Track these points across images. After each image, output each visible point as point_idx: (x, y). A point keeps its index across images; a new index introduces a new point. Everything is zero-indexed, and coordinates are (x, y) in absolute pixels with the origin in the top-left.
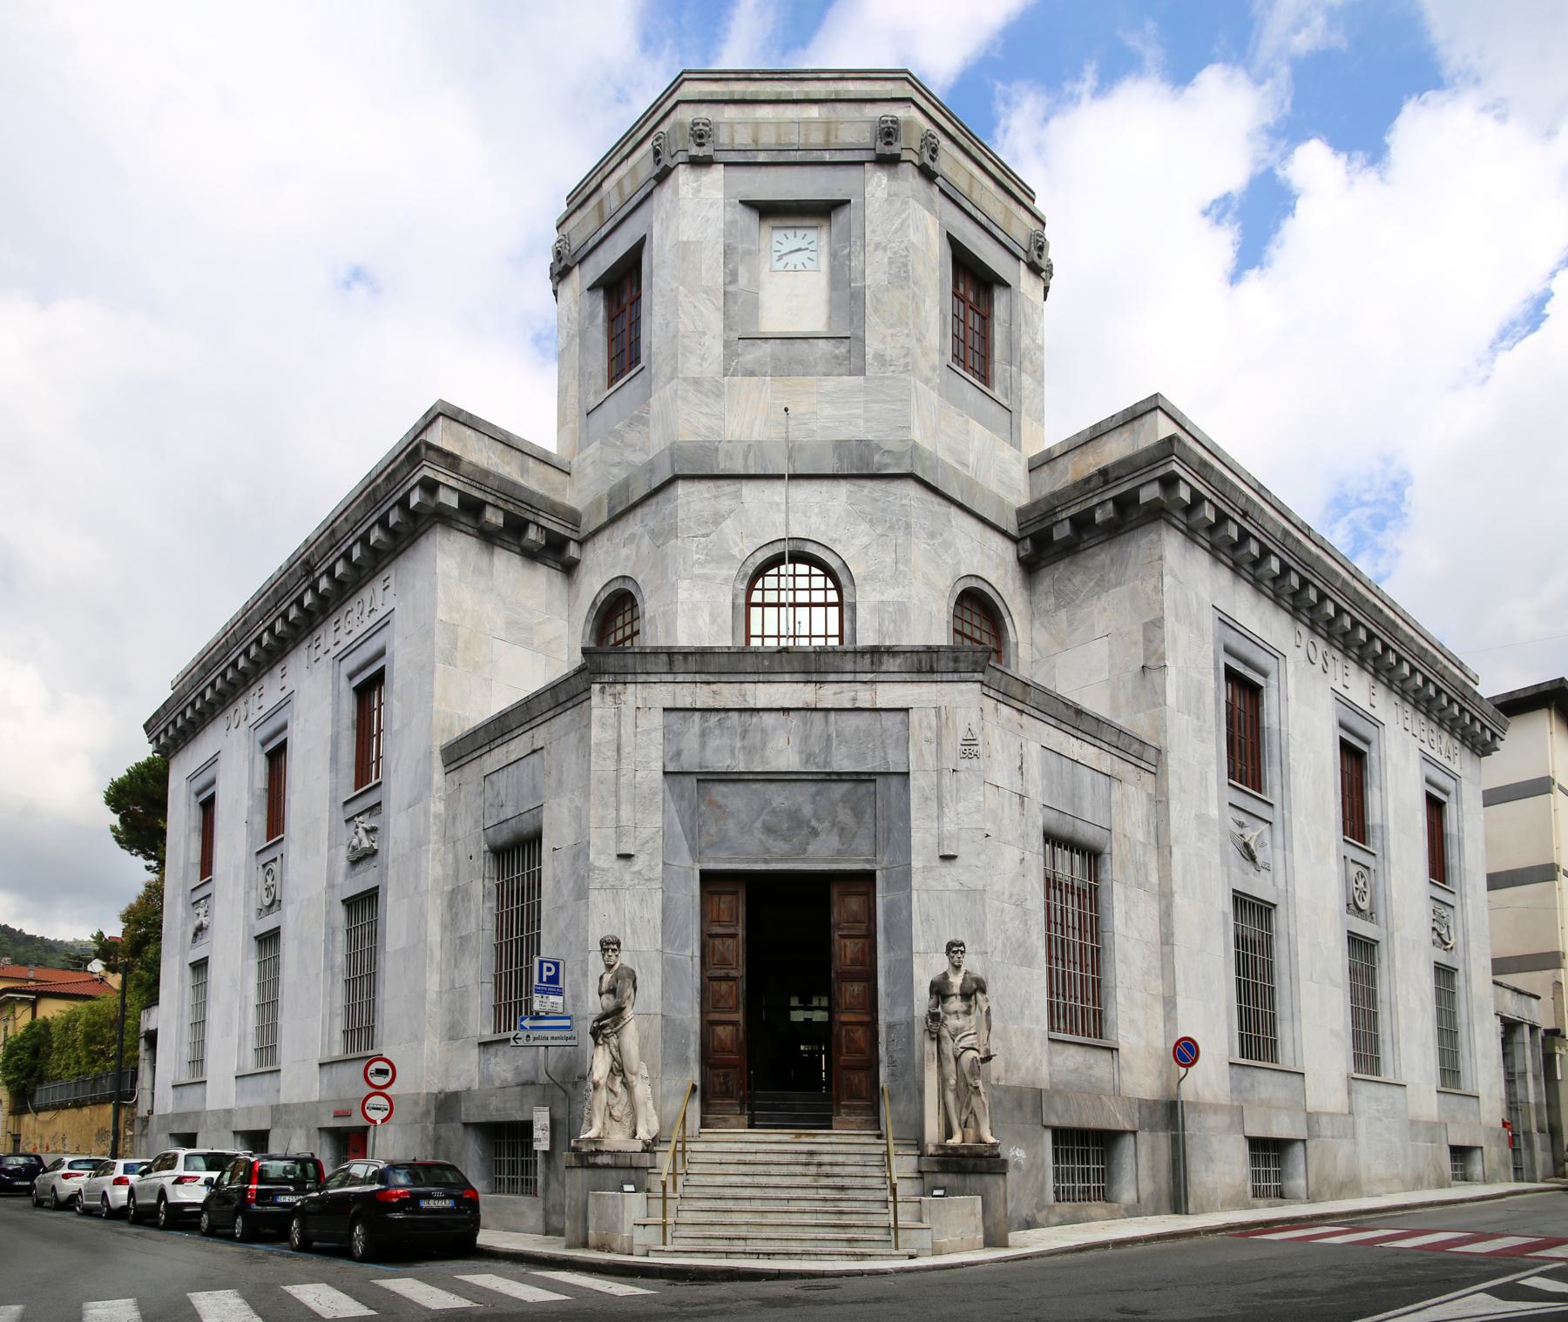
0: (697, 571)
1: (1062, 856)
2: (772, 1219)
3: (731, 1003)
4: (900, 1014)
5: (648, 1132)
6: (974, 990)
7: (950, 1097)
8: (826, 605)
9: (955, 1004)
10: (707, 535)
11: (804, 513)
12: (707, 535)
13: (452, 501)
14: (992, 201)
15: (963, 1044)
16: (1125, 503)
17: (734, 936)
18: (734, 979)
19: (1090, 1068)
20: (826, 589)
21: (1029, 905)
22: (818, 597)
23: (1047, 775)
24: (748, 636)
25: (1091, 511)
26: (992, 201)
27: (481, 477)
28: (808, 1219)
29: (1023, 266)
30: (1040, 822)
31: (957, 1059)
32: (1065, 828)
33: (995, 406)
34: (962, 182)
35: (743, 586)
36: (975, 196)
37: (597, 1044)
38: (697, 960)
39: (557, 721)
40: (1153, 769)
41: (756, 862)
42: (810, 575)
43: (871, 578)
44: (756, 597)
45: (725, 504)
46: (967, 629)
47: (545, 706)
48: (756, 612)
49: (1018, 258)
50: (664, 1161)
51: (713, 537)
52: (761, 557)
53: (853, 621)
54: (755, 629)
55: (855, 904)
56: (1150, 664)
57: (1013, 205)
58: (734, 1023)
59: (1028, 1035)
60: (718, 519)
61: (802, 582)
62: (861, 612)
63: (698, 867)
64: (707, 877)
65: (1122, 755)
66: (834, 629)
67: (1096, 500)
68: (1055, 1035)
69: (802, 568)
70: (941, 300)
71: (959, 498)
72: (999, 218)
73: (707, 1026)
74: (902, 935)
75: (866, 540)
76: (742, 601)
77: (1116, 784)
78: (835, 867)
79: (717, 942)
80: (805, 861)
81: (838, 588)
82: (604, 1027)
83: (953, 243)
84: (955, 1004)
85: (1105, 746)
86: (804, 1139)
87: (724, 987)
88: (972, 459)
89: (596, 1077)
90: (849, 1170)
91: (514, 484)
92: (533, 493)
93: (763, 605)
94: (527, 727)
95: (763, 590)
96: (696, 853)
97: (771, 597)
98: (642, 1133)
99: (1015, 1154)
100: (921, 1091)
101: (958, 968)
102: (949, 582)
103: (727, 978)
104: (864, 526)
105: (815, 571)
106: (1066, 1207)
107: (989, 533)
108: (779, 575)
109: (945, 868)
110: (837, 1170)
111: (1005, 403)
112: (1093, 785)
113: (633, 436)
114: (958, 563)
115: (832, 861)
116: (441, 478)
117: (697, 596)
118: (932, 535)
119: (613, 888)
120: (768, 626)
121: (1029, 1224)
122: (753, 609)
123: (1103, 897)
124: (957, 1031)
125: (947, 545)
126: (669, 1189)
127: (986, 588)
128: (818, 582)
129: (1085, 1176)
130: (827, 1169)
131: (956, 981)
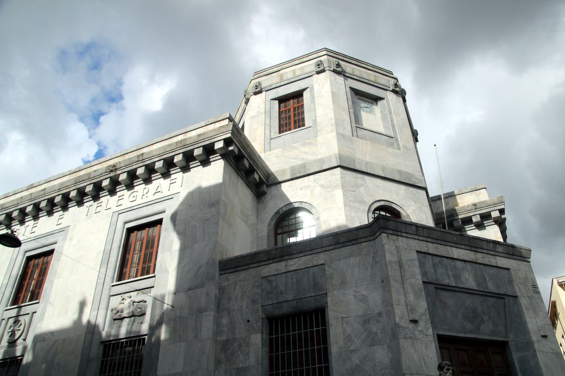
0: (351, 204)
11: (390, 192)
12: (354, 191)
39: (337, 251)
41: (460, 333)
51: (356, 192)
60: (358, 186)
63: (435, 332)
75: (414, 208)
78: (493, 338)
94: (309, 253)
113: (306, 149)
116: (235, 140)
117: (353, 214)
119: (410, 338)
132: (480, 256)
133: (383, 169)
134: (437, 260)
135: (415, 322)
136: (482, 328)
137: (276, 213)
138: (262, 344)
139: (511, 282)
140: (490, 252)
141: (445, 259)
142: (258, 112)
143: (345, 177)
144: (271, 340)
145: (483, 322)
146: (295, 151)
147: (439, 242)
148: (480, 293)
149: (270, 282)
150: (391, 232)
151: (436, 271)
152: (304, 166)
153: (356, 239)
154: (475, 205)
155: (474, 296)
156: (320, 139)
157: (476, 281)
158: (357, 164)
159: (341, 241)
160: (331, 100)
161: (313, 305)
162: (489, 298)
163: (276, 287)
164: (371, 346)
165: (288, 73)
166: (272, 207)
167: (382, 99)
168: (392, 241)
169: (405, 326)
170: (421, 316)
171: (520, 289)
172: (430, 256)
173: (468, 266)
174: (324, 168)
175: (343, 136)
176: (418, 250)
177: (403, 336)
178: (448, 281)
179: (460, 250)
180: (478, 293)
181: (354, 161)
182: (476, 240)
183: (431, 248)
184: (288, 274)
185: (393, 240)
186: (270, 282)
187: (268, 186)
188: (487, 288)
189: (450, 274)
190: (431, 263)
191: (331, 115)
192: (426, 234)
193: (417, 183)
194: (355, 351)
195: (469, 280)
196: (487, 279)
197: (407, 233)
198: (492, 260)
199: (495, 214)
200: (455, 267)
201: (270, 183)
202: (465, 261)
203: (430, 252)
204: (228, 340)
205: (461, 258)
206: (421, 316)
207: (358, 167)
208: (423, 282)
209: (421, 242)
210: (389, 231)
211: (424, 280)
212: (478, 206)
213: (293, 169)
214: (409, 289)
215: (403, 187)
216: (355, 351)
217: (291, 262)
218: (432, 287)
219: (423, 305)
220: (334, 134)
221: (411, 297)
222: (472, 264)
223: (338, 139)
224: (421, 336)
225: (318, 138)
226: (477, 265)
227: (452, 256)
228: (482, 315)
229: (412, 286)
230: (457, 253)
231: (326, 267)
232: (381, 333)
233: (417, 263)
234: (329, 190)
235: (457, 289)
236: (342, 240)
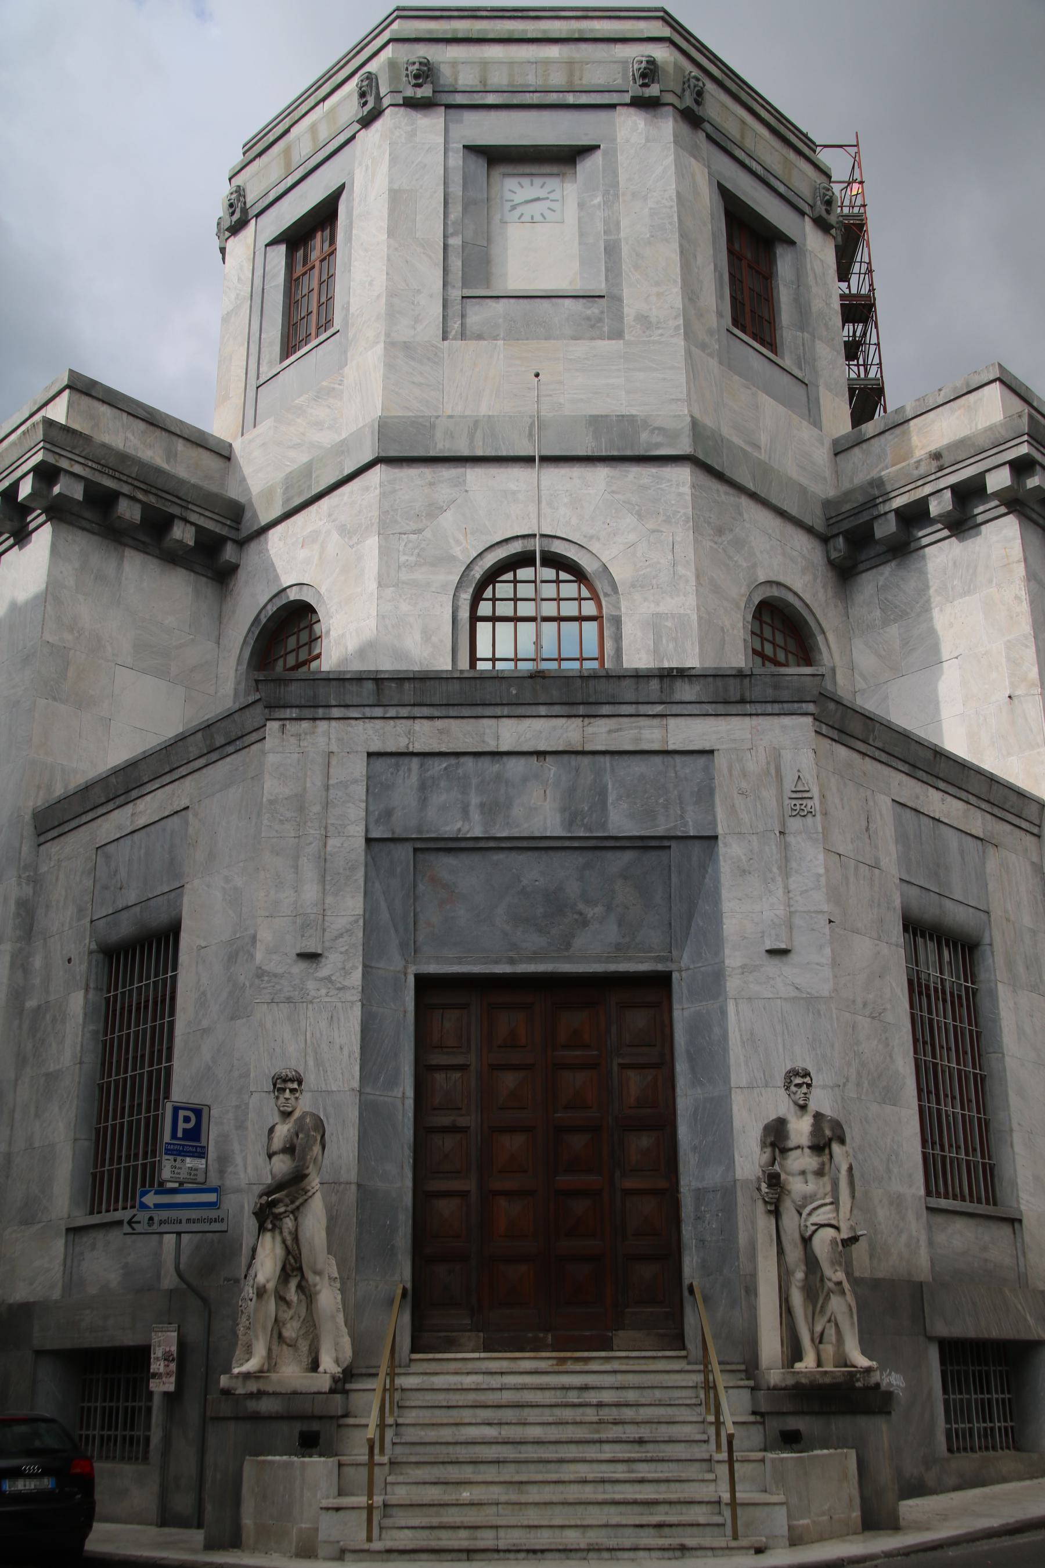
0: (404, 576)
1: (928, 950)
2: (534, 1494)
4: (713, 1176)
5: (337, 1361)
6: (827, 1138)
7: (797, 1298)
8: (580, 619)
9: (801, 1161)
10: (419, 531)
12: (419, 531)
13: (77, 492)
14: (770, 153)
15: (815, 1219)
16: (970, 493)
17: (463, 1068)
18: (464, 1130)
19: (985, 1249)
20: (580, 599)
21: (889, 1017)
22: (569, 609)
23: (902, 838)
24: (473, 659)
25: (924, 502)
26: (770, 153)
27: (117, 463)
28: (588, 1492)
29: (808, 224)
30: (897, 903)
31: (806, 1241)
32: (929, 909)
33: (786, 379)
34: (732, 128)
35: (466, 596)
36: (749, 144)
37: (262, 1229)
38: (410, 1103)
40: (1036, 830)
41: (497, 962)
42: (558, 581)
43: (638, 584)
44: (484, 609)
45: (444, 492)
46: (769, 650)
47: (194, 752)
48: (484, 629)
49: (803, 214)
50: (368, 1402)
51: (428, 534)
52: (491, 560)
53: (618, 638)
54: (483, 650)
55: (638, 1020)
56: (1018, 692)
57: (792, 155)
58: (464, 1195)
59: (897, 1202)
60: (434, 511)
61: (549, 591)
62: (630, 629)
63: (412, 970)
64: (425, 984)
65: (996, 811)
66: (591, 648)
67: (927, 490)
68: (934, 1202)
69: (549, 573)
70: (715, 256)
71: (751, 486)
72: (777, 169)
73: (422, 1197)
74: (712, 1062)
75: (632, 537)
76: (464, 614)
77: (991, 850)
78: (612, 967)
79: (440, 1077)
80: (569, 959)
81: (595, 597)
82: (274, 1204)
83: (726, 194)
84: (801, 1161)
85: (972, 799)
86: (570, 1366)
87: (449, 1142)
88: (764, 439)
89: (261, 1279)
90: (645, 1413)
91: (159, 471)
92: (182, 482)
93: (494, 619)
94: (167, 779)
95: (494, 600)
96: (412, 949)
97: (504, 609)
98: (328, 1363)
99: (894, 1381)
100: (751, 1290)
101: (803, 1108)
102: (744, 590)
103: (453, 1129)
104: (630, 520)
105: (564, 576)
106: (968, 1462)
107: (791, 530)
108: (515, 582)
109: (773, 967)
110: (628, 1413)
111: (799, 375)
112: (962, 852)
114: (754, 566)
115: (608, 960)
117: (405, 607)
118: (720, 531)
119: (289, 1000)
120: (502, 645)
121: (917, 1489)
122: (480, 625)
123: (984, 1002)
124: (807, 1199)
125: (739, 544)
126: (377, 1450)
127: (791, 598)
128: (569, 590)
129: (986, 1410)
130: (607, 1414)
131: (800, 1129)
132: (604, 729)
133: (538, 425)
134: (438, 766)
135: (311, 957)
136: (578, 942)
137: (252, 625)
138: (85, 1014)
139: (706, 794)
140: (644, 709)
141: (469, 762)
142: (237, 298)
143: (394, 491)
144: (108, 1000)
145: (584, 922)
146: (299, 420)
147: (452, 712)
148: (576, 844)
149: (108, 857)
150: (294, 713)
151: (424, 802)
152: (307, 471)
153: (243, 736)
154: (937, 456)
155: (551, 853)
156: (350, 373)
157: (563, 810)
158: (439, 435)
159: (218, 744)
160: (385, 224)
161: (159, 917)
162: (609, 855)
163: (116, 872)
164: (232, 1019)
165: (302, 142)
166: (251, 601)
167: (589, 149)
168: (293, 740)
169: (280, 970)
170: (336, 938)
171: (732, 810)
172: (415, 762)
173: (551, 768)
174: (347, 472)
175: (407, 347)
176: (371, 750)
178: (459, 824)
179: (528, 722)
180: (567, 844)
181: (433, 426)
182: (591, 683)
183: (425, 735)
184: (136, 835)
185: (298, 736)
186: (108, 857)
187: (242, 543)
188: (604, 826)
189: (474, 800)
190: (414, 779)
191: (381, 282)
192: (408, 698)
193: (658, 445)
194: (206, 1031)
195: (539, 811)
196: (611, 798)
197: (347, 706)
198: (650, 734)
199: (999, 480)
200: (498, 778)
201: (244, 533)
202: (541, 754)
203: (418, 747)
204: (39, 1007)
205: (525, 749)
206: (336, 938)
207: (441, 447)
208: (369, 841)
209: (392, 722)
210: (288, 713)
211: (375, 834)
212: (946, 460)
213: (289, 482)
214: (309, 870)
215: (601, 474)
216: (206, 1031)
217: (141, 805)
218: (404, 853)
219: (350, 906)
220: (379, 349)
221: (310, 892)
222: (566, 757)
223: (390, 366)
224: (323, 991)
225: (346, 370)
226: (586, 760)
227: (491, 747)
228: (581, 906)
229: (323, 860)
230: (510, 733)
231: (191, 816)
232: (250, 986)
233: (360, 790)
234: (355, 539)
235: (492, 844)
236: (220, 740)
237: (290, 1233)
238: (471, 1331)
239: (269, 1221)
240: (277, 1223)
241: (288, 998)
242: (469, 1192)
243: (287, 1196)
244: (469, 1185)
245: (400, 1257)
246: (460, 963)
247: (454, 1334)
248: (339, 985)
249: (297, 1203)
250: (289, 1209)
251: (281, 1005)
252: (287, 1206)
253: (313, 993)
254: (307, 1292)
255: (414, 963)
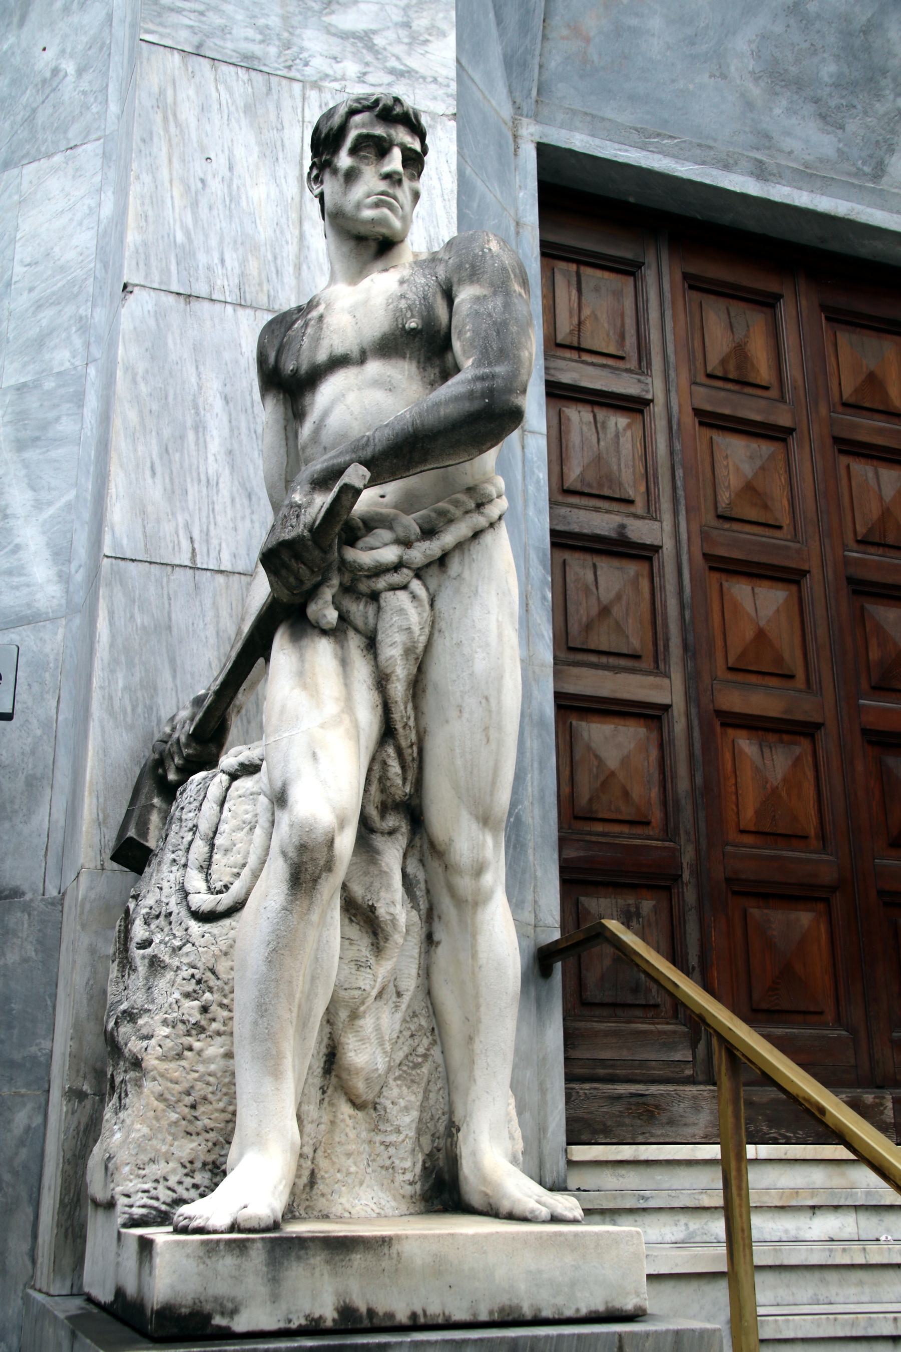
3: (635, 638)
17: (634, 406)
18: (645, 554)
41: (726, 167)
63: (531, 133)
80: (882, 199)
87: (612, 578)
96: (530, 82)
119: (248, 63)
177: (184, 39)
232: (80, 72)
237: (408, 651)
238: (691, 1081)
239: (328, 594)
240: (358, 610)
241: (246, 57)
242: (666, 708)
243: (408, 503)
244: (667, 690)
245: (530, 851)
246: (643, 147)
247: (653, 1089)
248: (393, 63)
249: (448, 538)
250: (419, 553)
251: (224, 68)
252: (406, 543)
253: (319, 64)
254: (439, 899)
255: (536, 117)
